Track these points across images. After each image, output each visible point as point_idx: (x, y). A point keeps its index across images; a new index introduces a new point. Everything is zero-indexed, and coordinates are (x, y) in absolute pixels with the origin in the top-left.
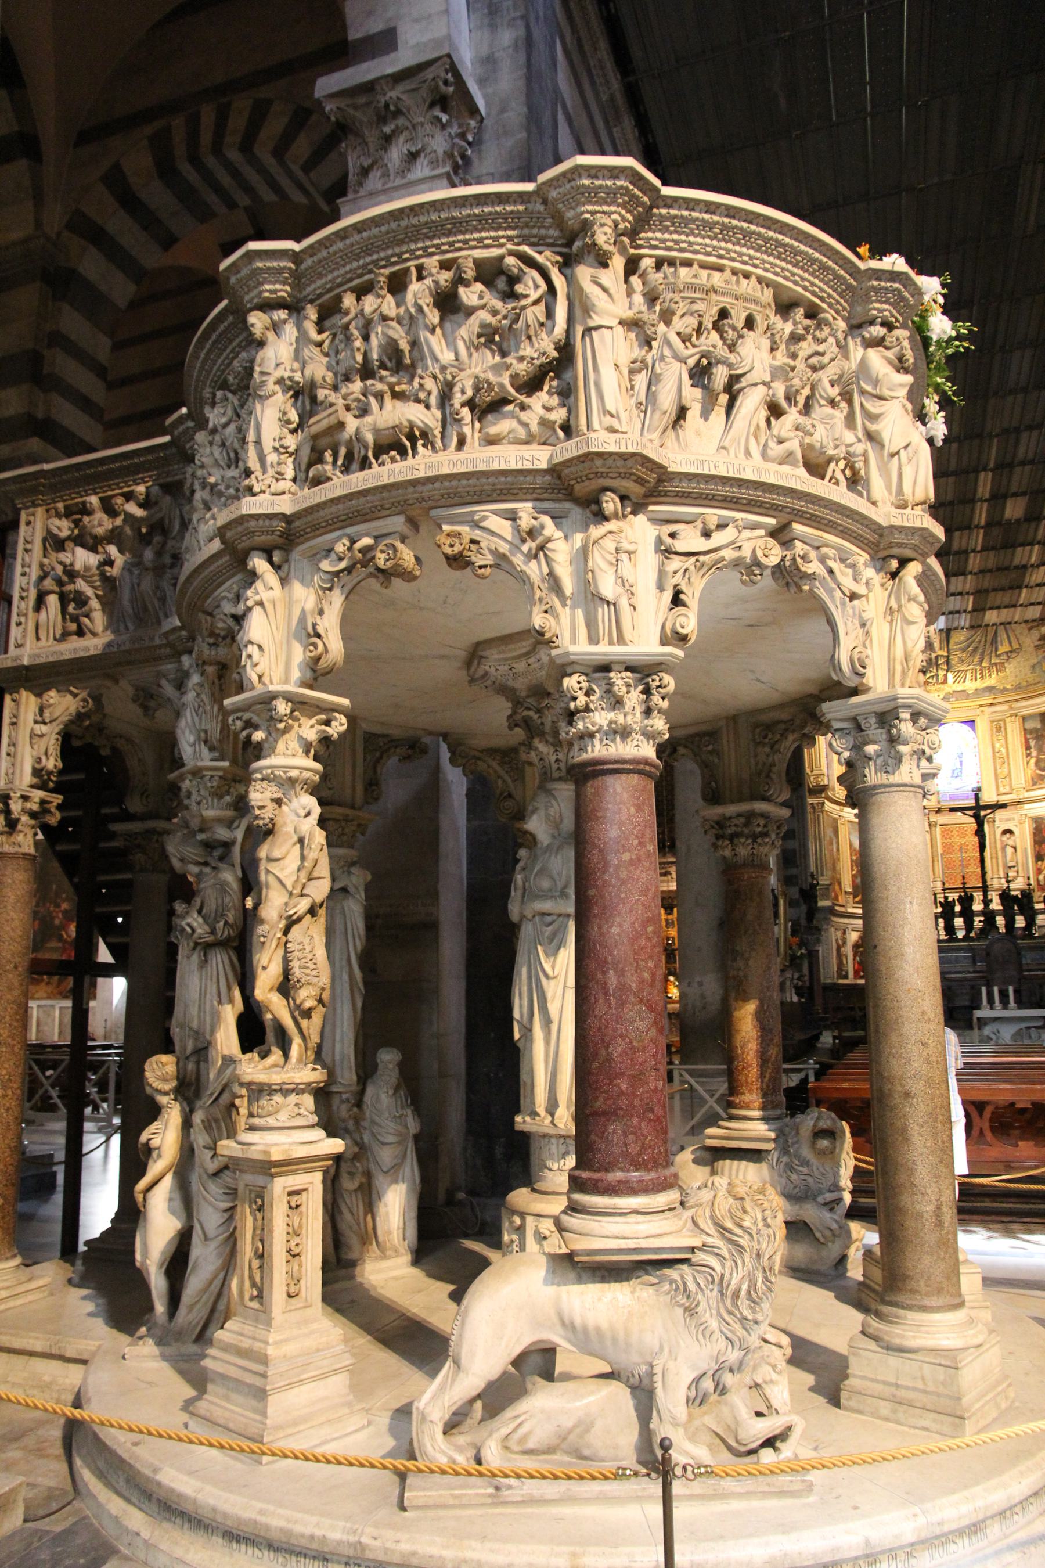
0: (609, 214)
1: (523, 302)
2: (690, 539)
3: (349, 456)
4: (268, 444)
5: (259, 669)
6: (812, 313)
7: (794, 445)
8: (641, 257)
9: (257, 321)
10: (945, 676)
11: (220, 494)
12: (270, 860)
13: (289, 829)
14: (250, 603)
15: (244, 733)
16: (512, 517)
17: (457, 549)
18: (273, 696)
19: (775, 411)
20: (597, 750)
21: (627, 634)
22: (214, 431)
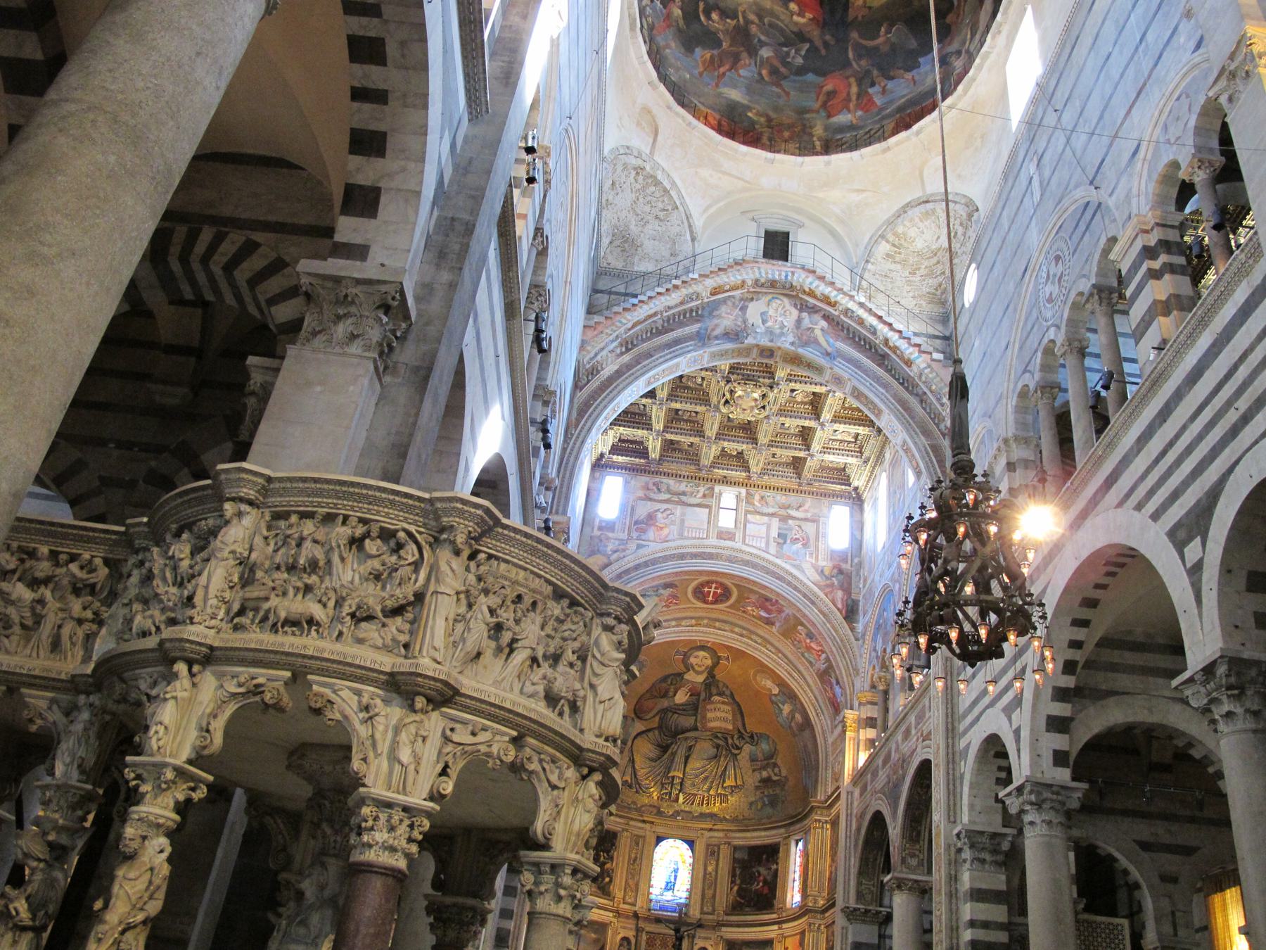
0: (467, 526)
1: (402, 563)
2: (462, 736)
3: (265, 619)
4: (213, 591)
5: (161, 743)
6: (574, 603)
7: (540, 689)
8: (481, 551)
9: (229, 507)
10: (678, 796)
11: (161, 601)
12: (124, 878)
13: (145, 859)
14: (168, 696)
15: (134, 783)
16: (358, 693)
17: (318, 705)
18: (165, 765)
19: (534, 660)
20: (371, 856)
21: (408, 789)
22: (173, 557)
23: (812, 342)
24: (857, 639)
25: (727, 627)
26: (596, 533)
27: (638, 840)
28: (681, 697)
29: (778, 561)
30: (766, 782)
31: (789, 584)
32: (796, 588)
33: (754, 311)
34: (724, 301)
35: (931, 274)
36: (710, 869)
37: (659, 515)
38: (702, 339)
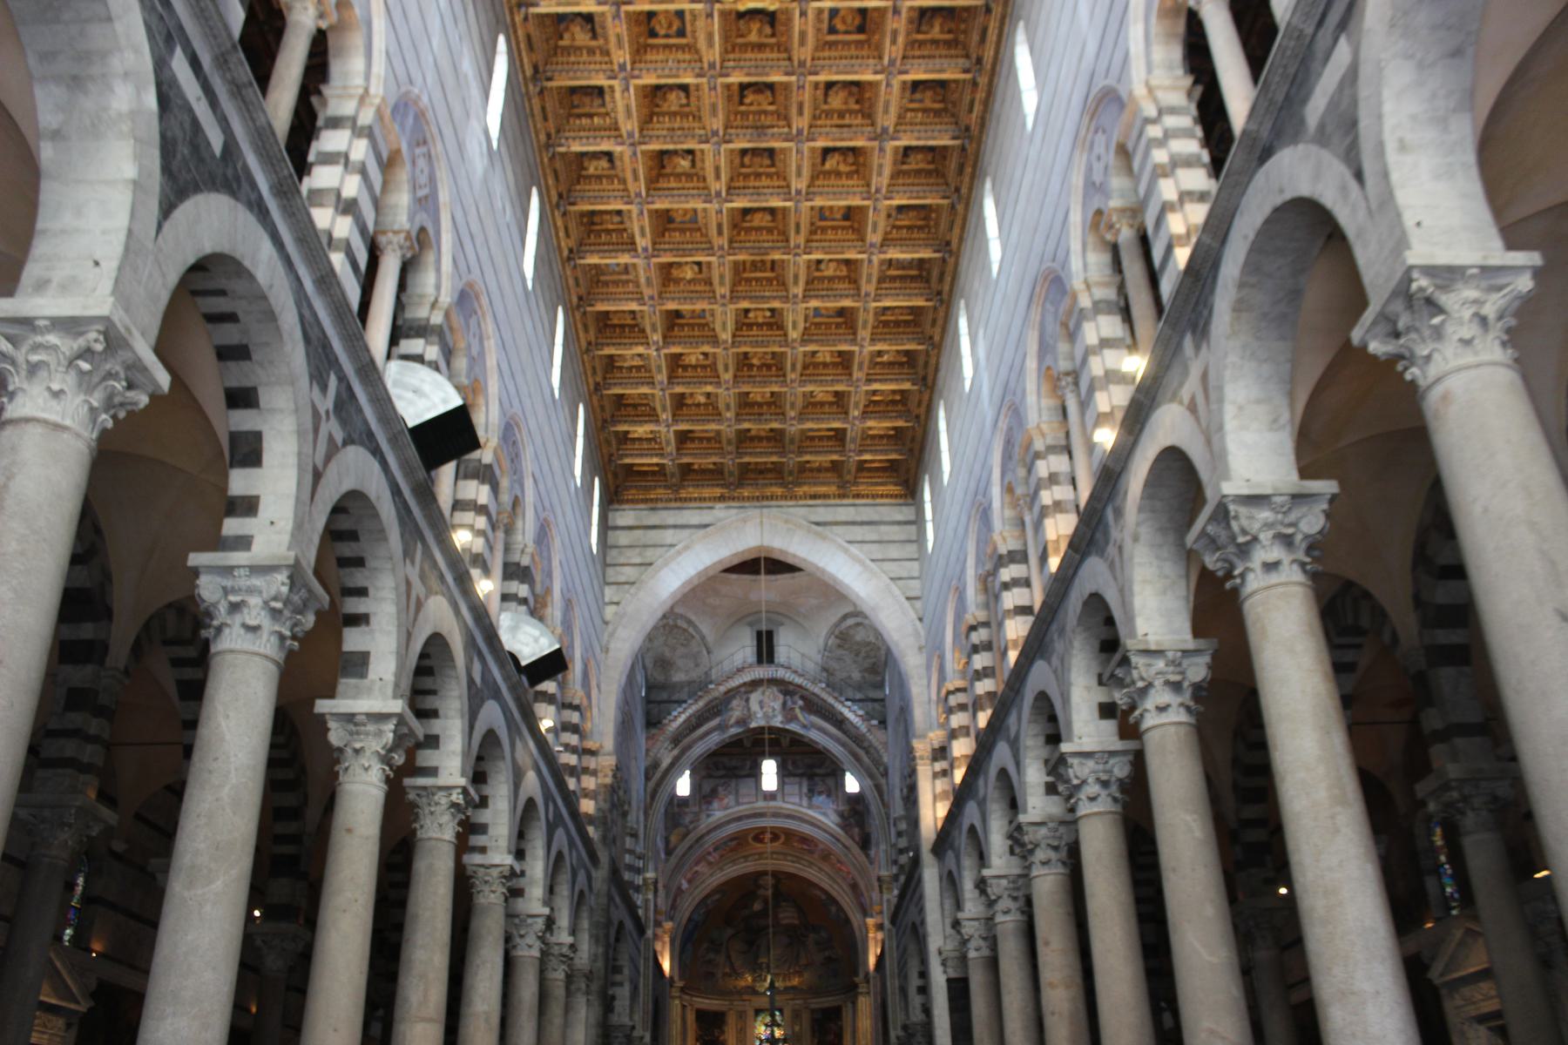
23: (794, 719)
24: (871, 863)
25: (781, 857)
26: (676, 809)
27: (742, 1015)
28: (757, 906)
29: (810, 812)
30: (829, 959)
31: (819, 828)
32: (825, 831)
33: (755, 697)
34: (734, 697)
35: (868, 657)
36: (797, 1028)
37: (720, 789)
38: (721, 728)
